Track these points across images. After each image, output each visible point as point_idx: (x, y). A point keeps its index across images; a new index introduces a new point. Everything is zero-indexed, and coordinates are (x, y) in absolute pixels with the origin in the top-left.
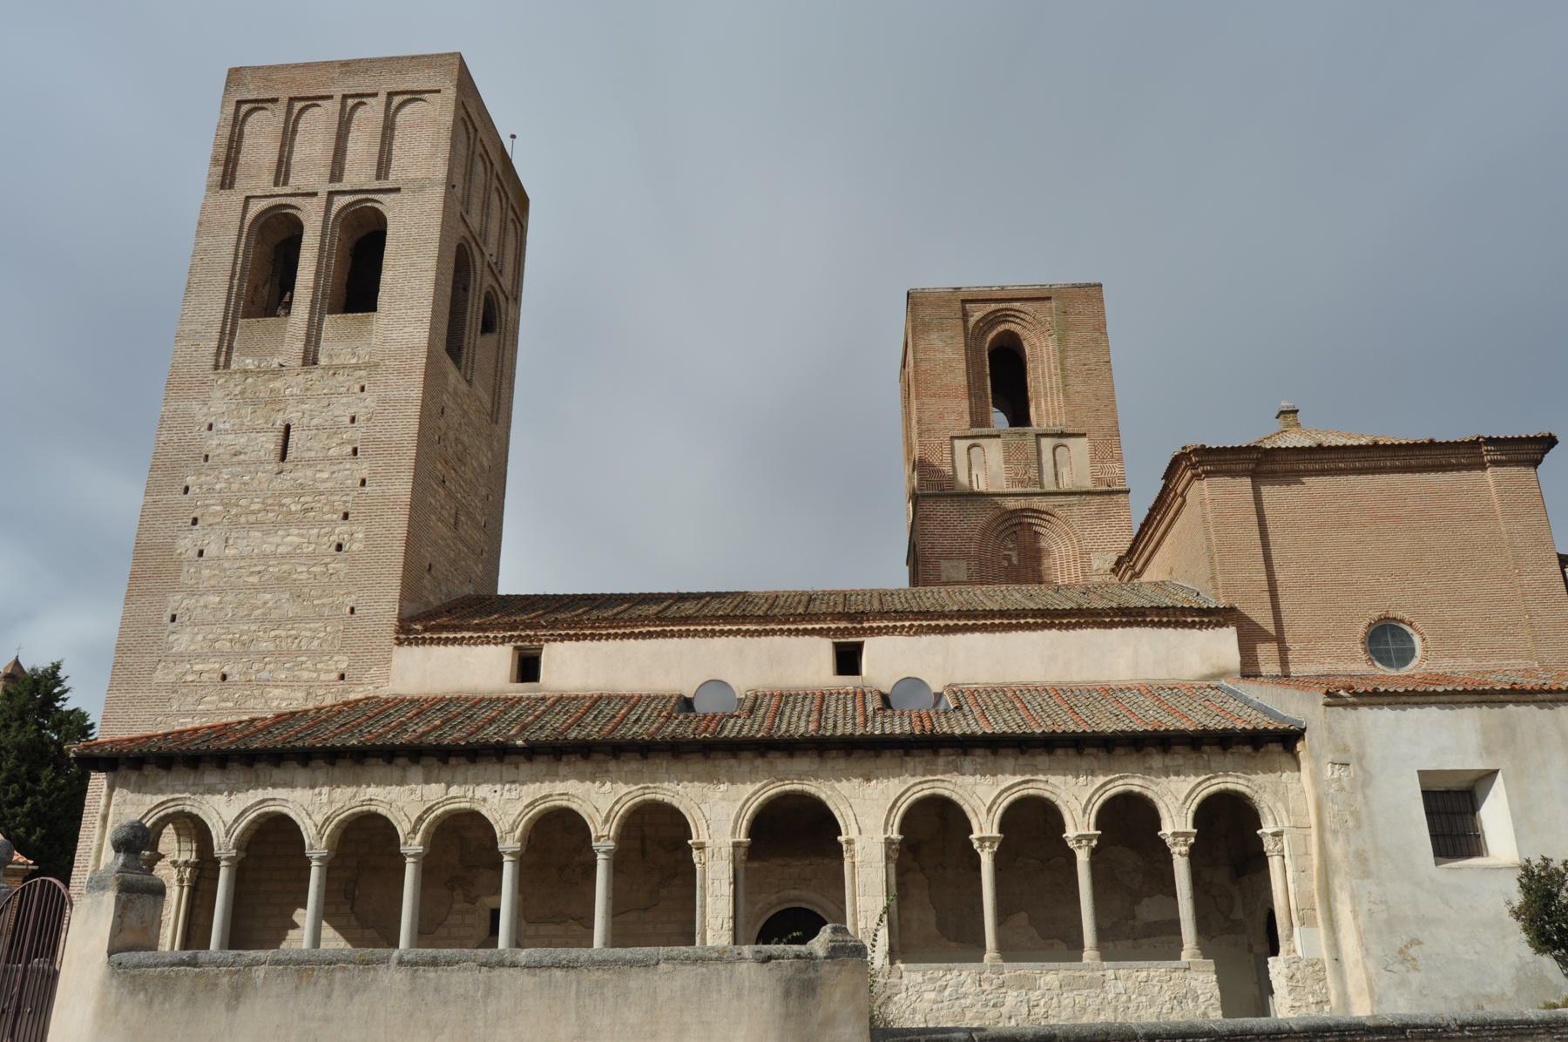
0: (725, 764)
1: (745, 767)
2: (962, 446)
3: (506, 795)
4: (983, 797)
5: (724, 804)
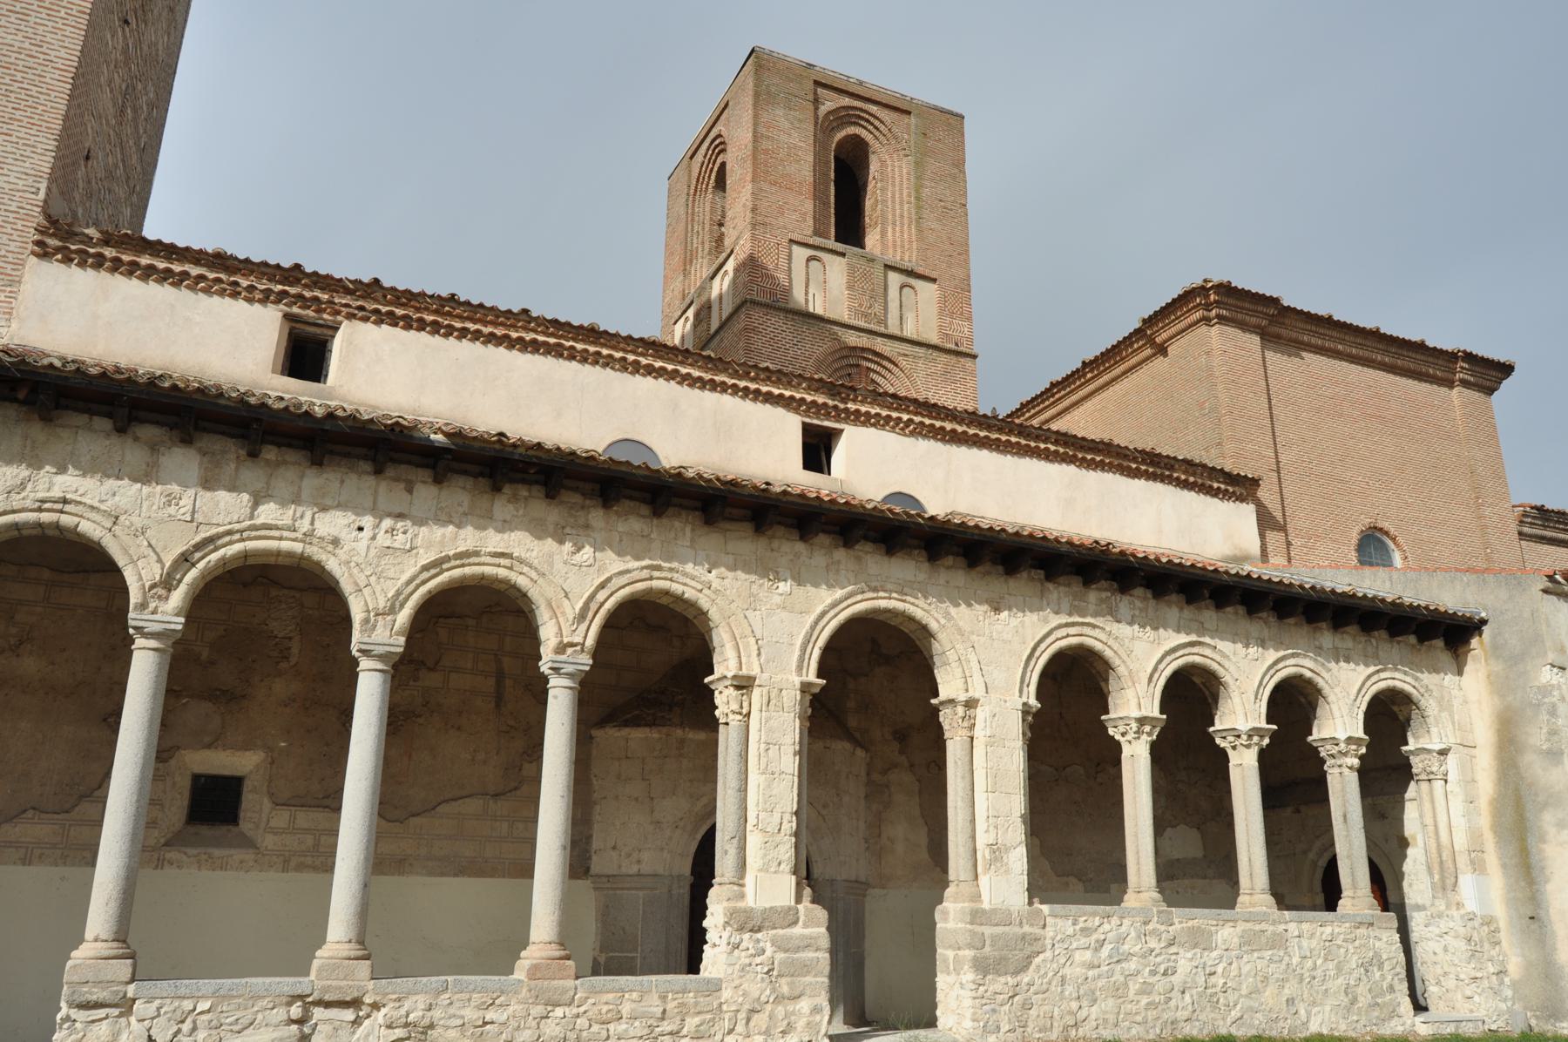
0: (790, 548)
1: (819, 559)
2: (800, 254)
3: (383, 540)
4: (1140, 657)
5: (784, 615)
